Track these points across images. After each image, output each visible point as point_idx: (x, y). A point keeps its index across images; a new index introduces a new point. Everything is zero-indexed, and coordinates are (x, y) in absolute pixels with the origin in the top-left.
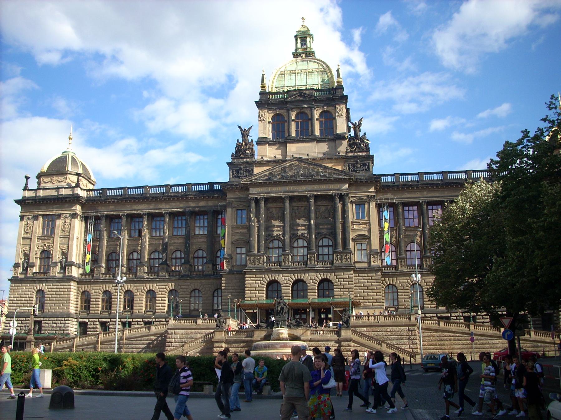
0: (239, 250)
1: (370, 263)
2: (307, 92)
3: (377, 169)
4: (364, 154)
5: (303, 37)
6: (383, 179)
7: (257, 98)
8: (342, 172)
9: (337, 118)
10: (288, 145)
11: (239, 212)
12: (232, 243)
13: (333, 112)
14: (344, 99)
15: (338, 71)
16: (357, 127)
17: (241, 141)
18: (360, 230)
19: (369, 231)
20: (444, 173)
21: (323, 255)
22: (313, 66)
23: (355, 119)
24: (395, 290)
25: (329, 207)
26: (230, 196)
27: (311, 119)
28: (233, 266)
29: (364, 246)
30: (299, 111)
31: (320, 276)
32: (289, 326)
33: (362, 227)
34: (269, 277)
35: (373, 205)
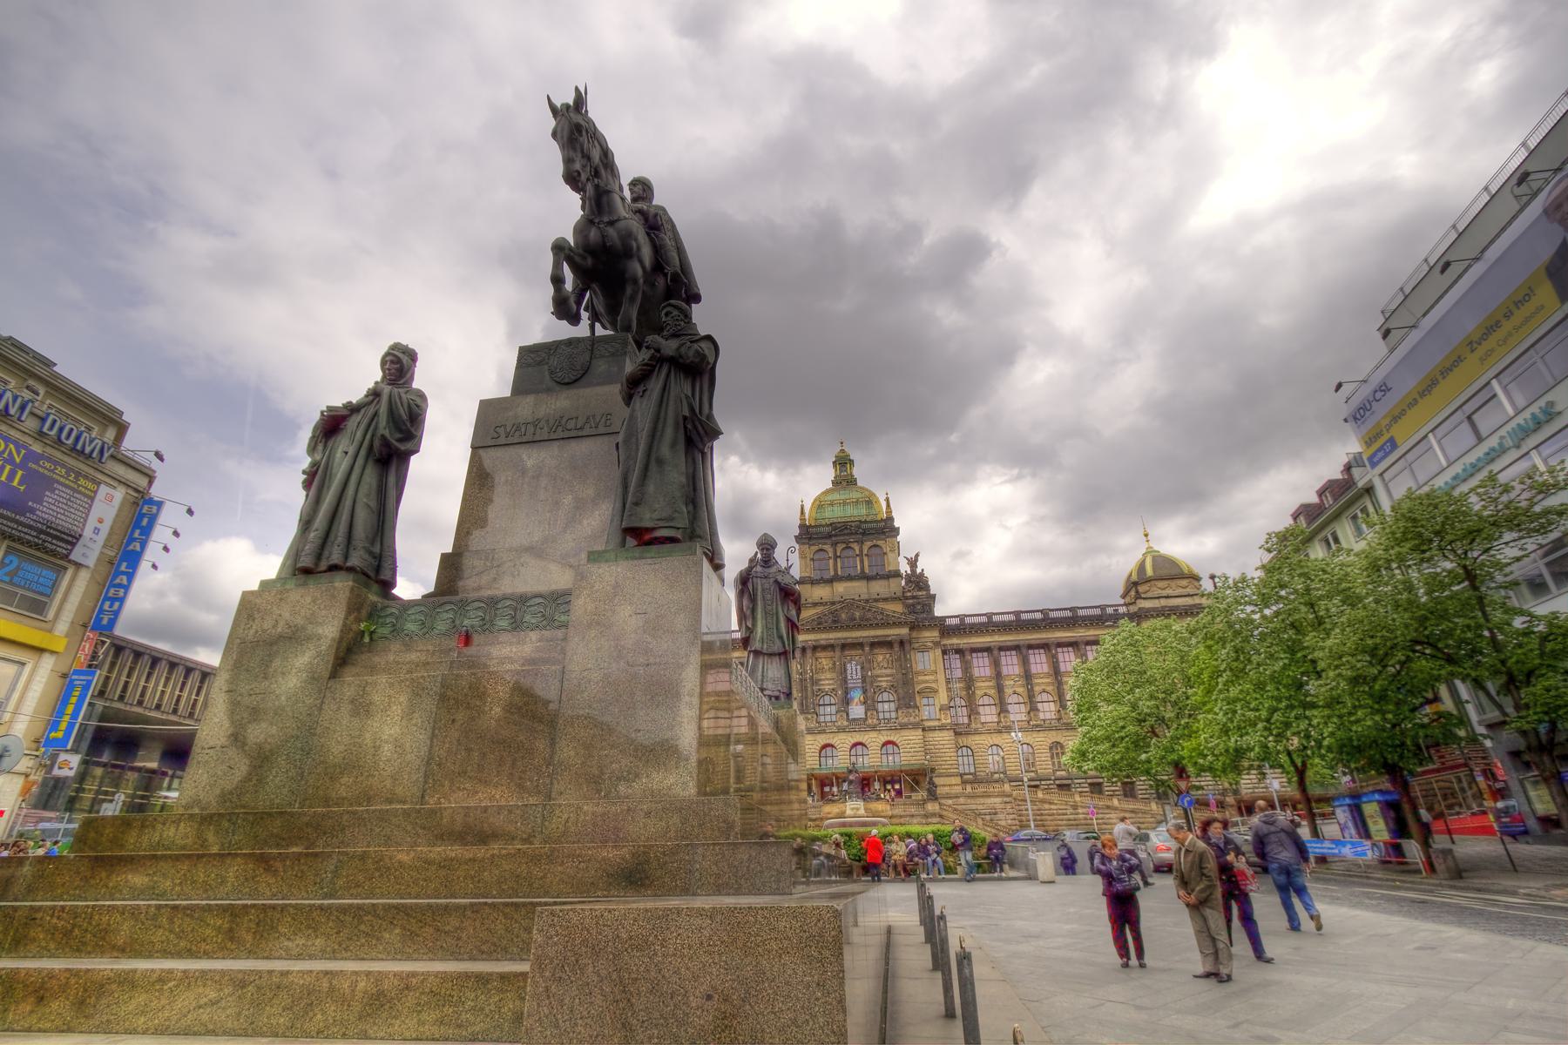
3: (939, 611)
6: (948, 622)
7: (797, 532)
9: (891, 555)
14: (896, 531)
15: (887, 500)
16: (913, 563)
20: (1017, 613)
22: (855, 495)
23: (907, 551)
31: (884, 739)
34: (822, 739)
35: (939, 652)
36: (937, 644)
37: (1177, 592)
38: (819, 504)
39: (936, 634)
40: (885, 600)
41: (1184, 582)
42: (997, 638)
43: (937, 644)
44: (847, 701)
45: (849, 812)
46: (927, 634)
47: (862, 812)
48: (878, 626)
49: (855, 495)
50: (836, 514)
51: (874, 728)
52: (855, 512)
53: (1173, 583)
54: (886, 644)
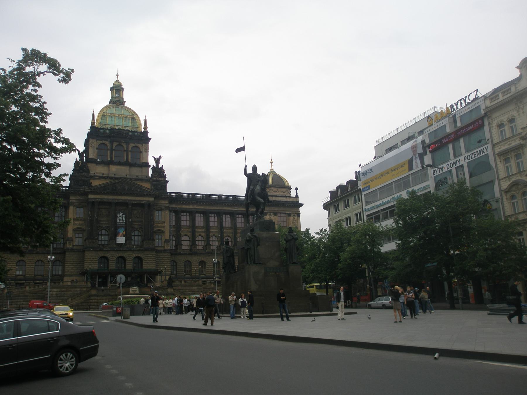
0: (77, 235)
1: (164, 247)
2: (124, 132)
4: (163, 179)
5: (117, 89)
8: (151, 189)
9: (144, 153)
10: (110, 166)
11: (78, 209)
12: (74, 230)
13: (141, 148)
15: (145, 120)
16: (157, 161)
17: (78, 160)
18: (159, 227)
19: (164, 227)
21: (135, 241)
24: (175, 264)
25: (140, 211)
26: (72, 198)
27: (127, 151)
28: (73, 246)
29: (160, 237)
30: (118, 144)
32: (139, 286)
33: (160, 225)
34: (101, 254)
35: (167, 212)
36: (167, 208)
37: (280, 195)
38: (103, 114)
39: (167, 202)
40: (142, 180)
41: (284, 190)
42: (196, 207)
43: (167, 208)
44: (116, 234)
45: (131, 292)
46: (162, 202)
47: (138, 292)
48: (137, 195)
49: (125, 113)
50: (114, 123)
51: (130, 250)
52: (125, 124)
53: (280, 190)
54: (141, 205)
